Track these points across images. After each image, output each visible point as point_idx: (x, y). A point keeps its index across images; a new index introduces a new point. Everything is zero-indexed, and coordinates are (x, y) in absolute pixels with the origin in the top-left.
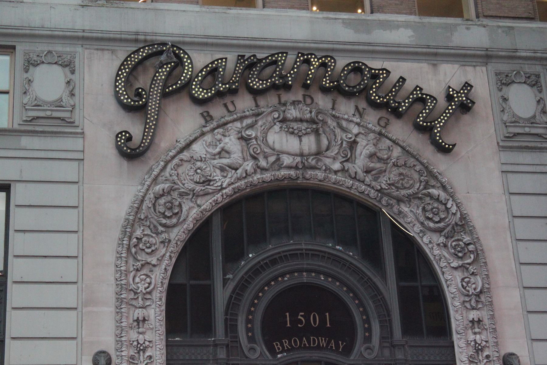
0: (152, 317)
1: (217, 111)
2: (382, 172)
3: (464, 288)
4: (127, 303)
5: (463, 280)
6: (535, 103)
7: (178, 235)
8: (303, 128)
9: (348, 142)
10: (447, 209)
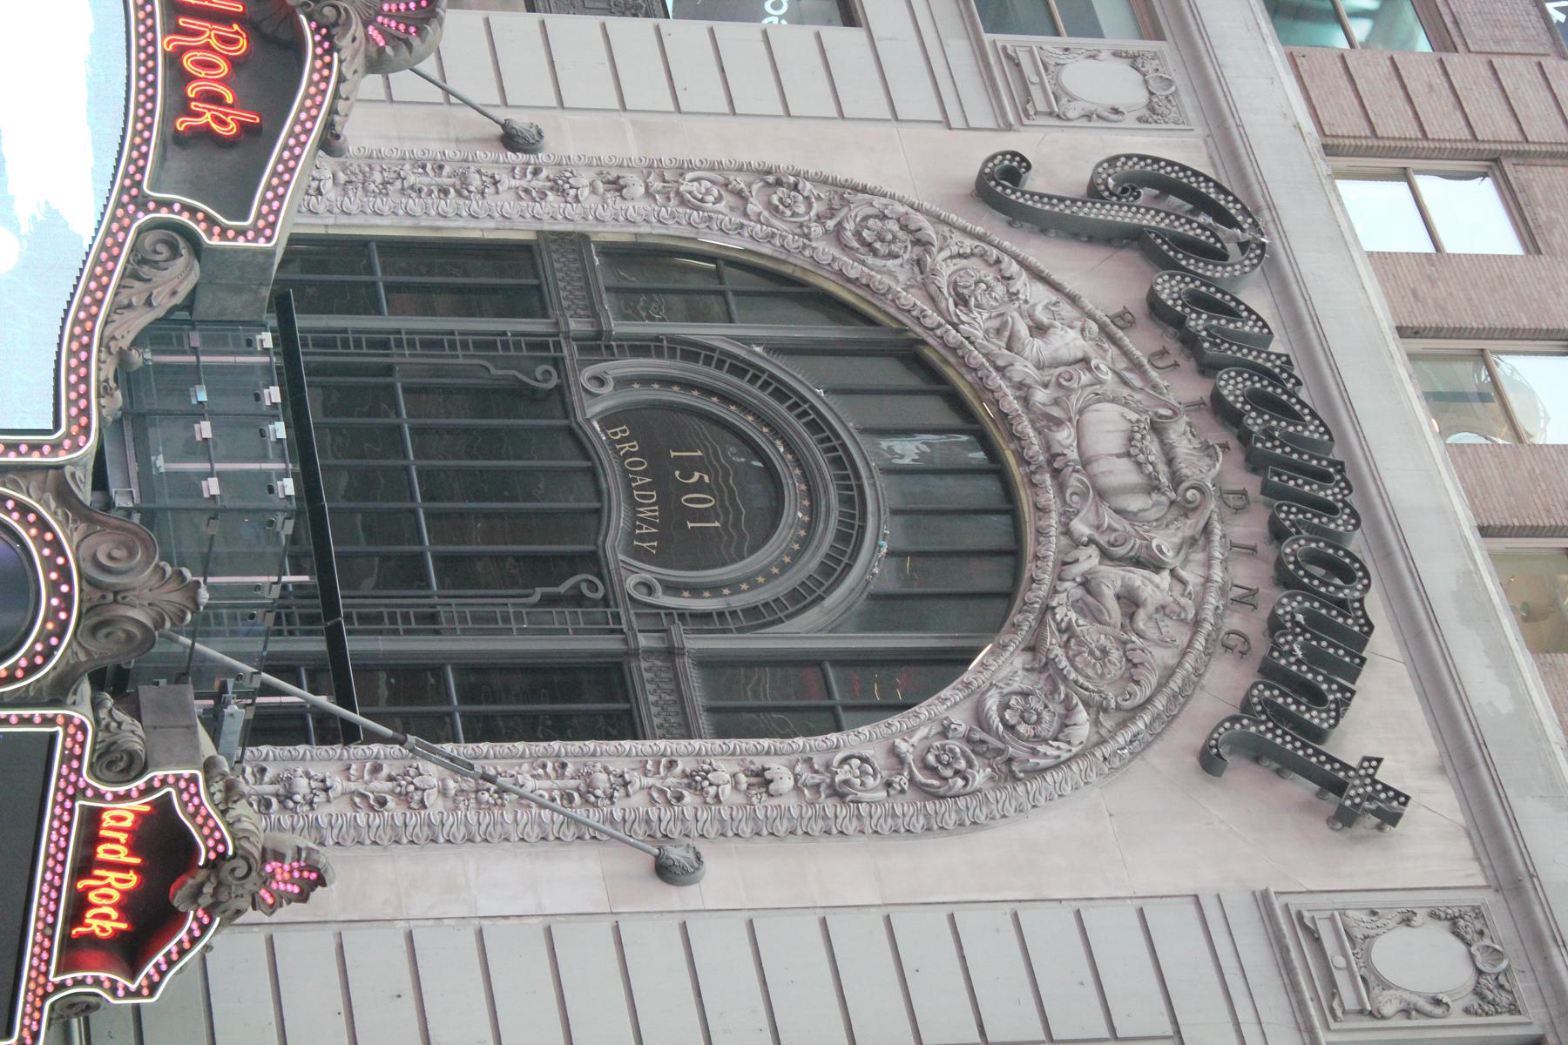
0: (630, 205)
1: (1142, 341)
2: (1096, 617)
3: (845, 760)
4: (651, 167)
5: (864, 760)
6: (1431, 989)
7: (826, 250)
8: (1152, 458)
9: (1149, 547)
10: (1045, 741)
